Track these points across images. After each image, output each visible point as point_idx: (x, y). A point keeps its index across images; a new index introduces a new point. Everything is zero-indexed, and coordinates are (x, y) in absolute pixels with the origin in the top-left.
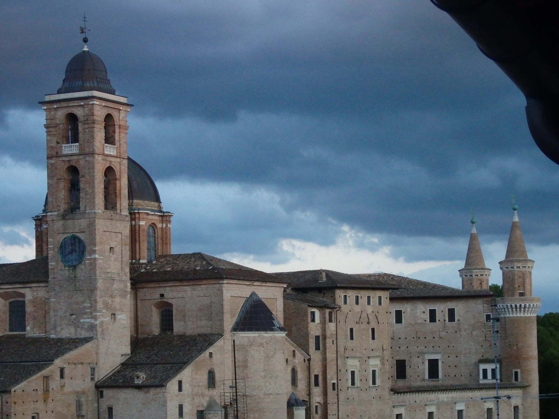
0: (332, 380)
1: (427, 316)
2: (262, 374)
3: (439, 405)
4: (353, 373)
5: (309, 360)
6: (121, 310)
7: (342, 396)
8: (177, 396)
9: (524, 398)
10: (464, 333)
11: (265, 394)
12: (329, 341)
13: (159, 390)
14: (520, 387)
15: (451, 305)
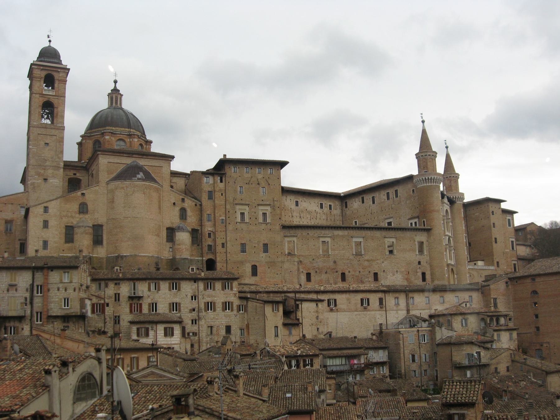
0: (220, 216)
1: (385, 197)
2: (123, 205)
3: (332, 238)
4: (242, 214)
5: (201, 205)
6: (54, 177)
7: (230, 227)
8: (42, 215)
9: (429, 237)
10: (402, 203)
11: (125, 218)
12: (217, 195)
13: (96, 224)
14: (425, 230)
15: (396, 188)
